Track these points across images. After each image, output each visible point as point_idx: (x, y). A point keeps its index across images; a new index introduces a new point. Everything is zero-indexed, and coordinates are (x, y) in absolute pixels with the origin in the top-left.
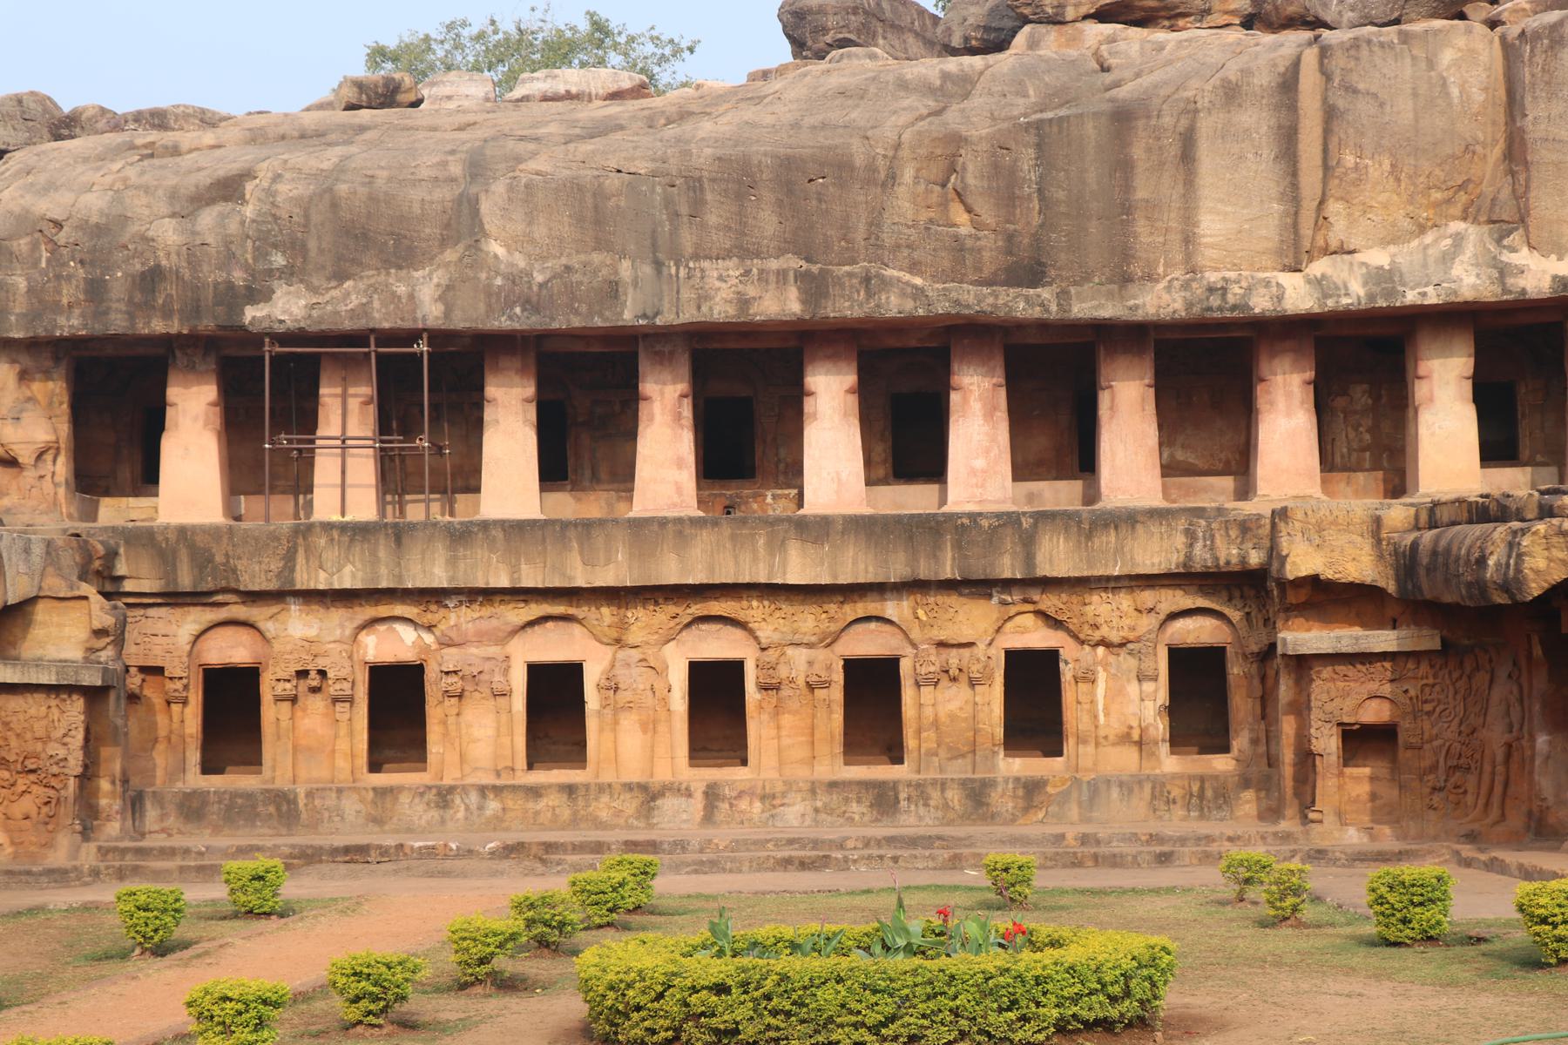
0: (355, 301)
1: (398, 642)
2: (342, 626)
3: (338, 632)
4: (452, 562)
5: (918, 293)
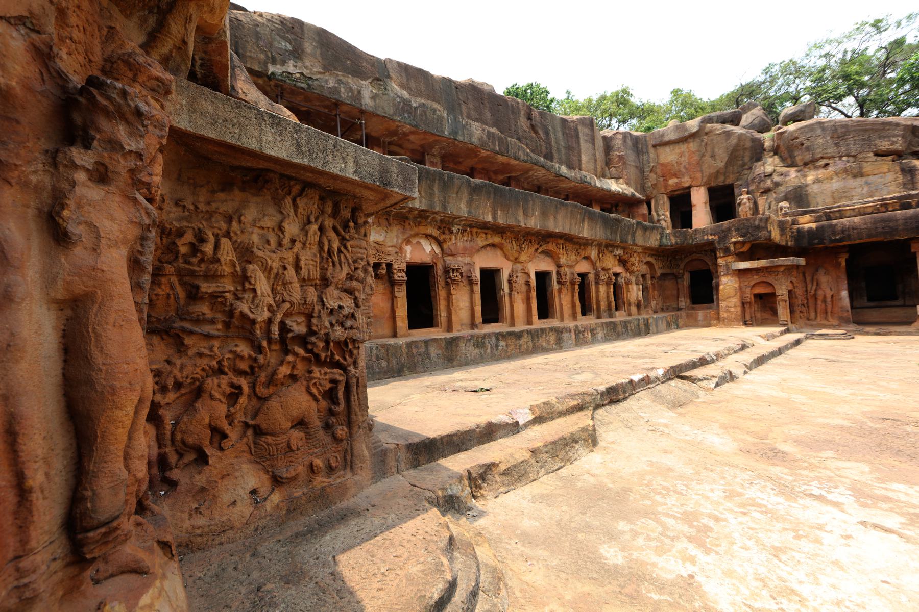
0: (331, 84)
1: (424, 251)
2: (397, 237)
3: (395, 240)
4: (470, 202)
5: (528, 155)
